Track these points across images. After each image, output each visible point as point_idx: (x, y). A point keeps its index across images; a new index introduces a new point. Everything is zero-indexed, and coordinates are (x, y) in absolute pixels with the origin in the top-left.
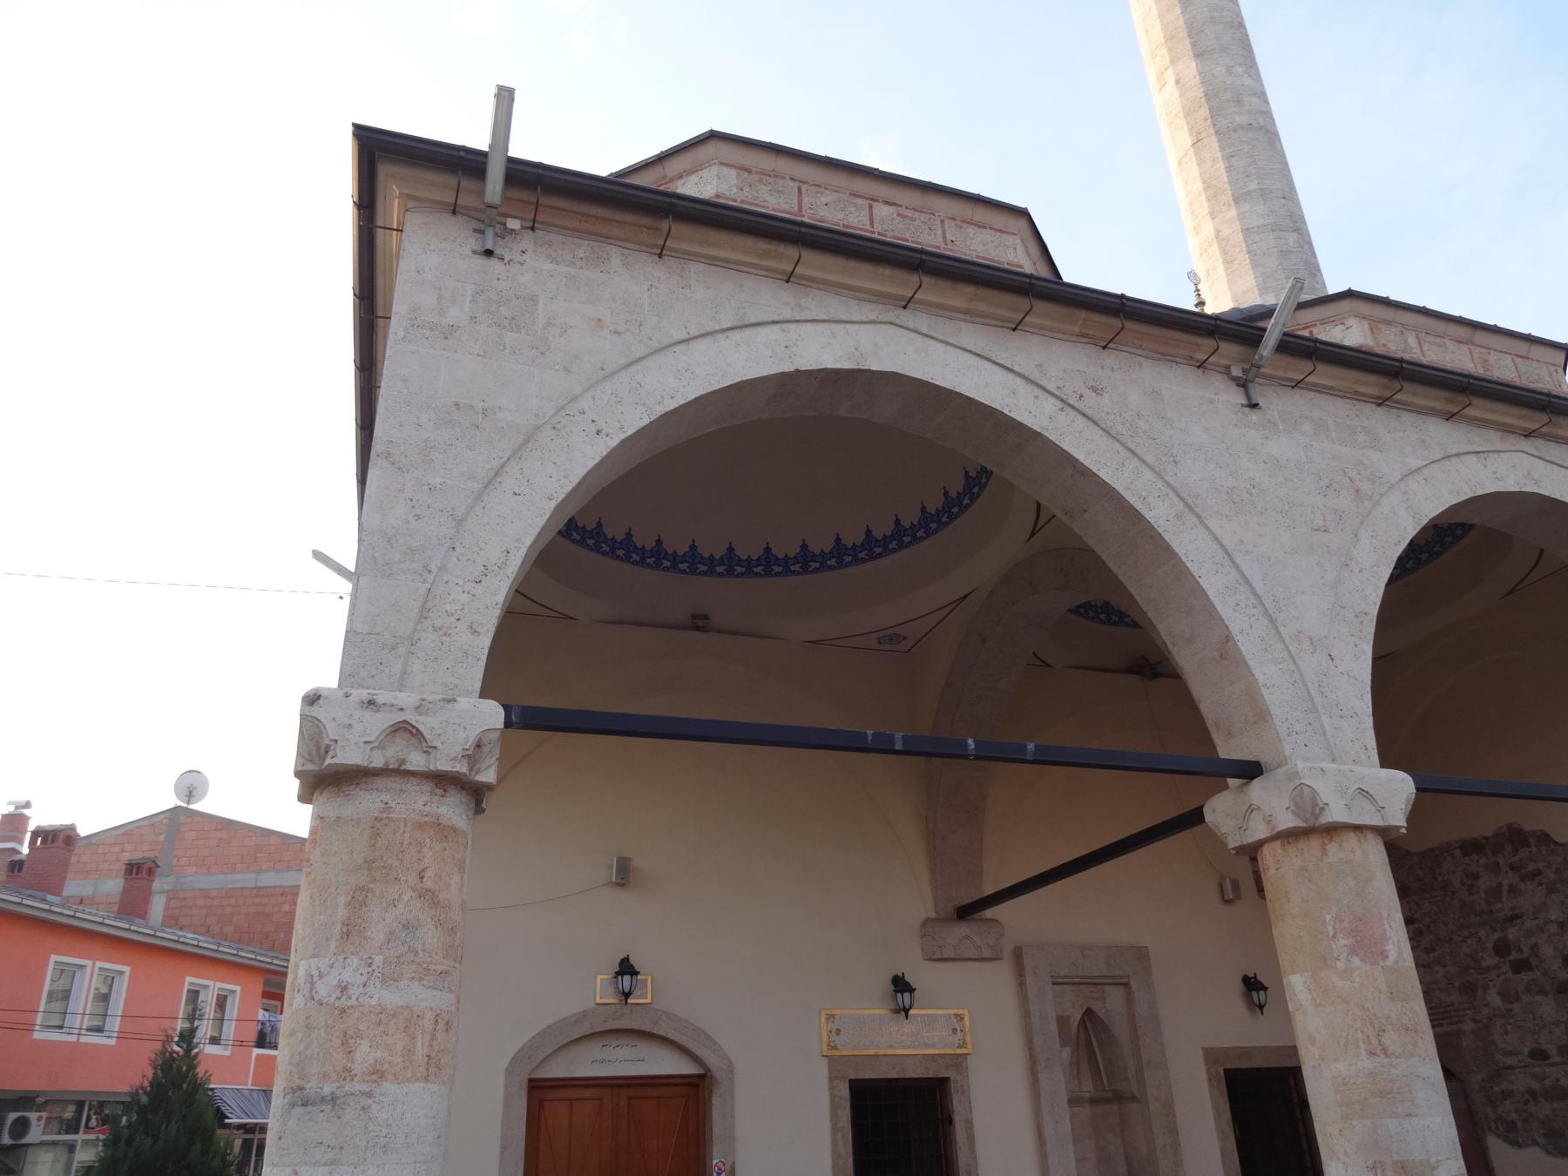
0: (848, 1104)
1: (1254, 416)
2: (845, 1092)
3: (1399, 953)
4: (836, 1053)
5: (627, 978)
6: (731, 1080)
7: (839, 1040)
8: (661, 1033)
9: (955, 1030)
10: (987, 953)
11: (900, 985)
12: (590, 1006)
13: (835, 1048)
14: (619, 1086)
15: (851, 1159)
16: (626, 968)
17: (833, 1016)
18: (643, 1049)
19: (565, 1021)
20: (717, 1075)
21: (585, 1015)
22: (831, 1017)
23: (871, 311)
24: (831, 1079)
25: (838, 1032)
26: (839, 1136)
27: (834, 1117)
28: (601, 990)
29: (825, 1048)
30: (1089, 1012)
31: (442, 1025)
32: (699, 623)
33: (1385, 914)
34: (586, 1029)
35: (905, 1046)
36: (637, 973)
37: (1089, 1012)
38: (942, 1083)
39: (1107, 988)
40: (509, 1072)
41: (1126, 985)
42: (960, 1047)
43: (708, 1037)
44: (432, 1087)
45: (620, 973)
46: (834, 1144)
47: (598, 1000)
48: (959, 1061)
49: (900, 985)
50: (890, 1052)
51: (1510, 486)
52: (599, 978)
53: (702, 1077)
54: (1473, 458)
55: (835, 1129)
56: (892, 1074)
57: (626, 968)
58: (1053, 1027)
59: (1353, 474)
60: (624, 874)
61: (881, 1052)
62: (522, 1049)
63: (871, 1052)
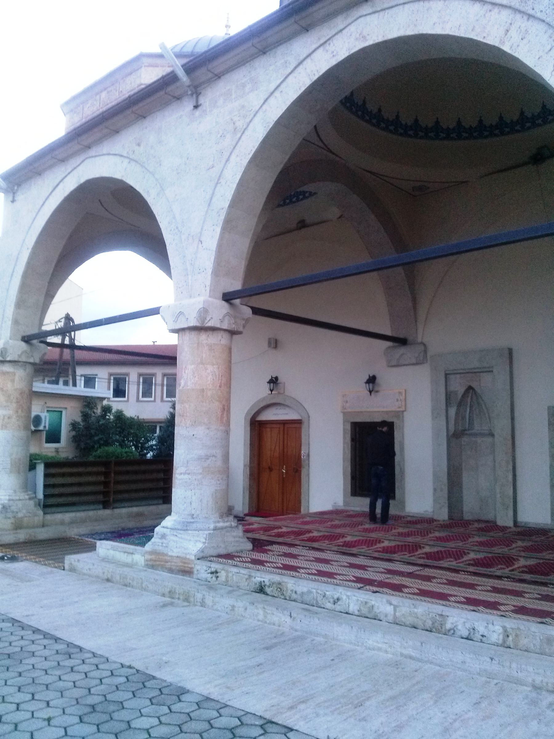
0: (350, 433)
1: (197, 113)
2: (349, 427)
3: (186, 383)
4: (345, 411)
5: (272, 384)
8: (286, 404)
9: (397, 400)
10: (414, 361)
11: (372, 380)
13: (345, 409)
15: (350, 455)
16: (274, 381)
18: (287, 410)
20: (303, 420)
23: (82, 157)
24: (344, 422)
27: (344, 438)
30: (470, 388)
31: (6, 418)
32: (302, 225)
33: (184, 367)
35: (375, 408)
37: (470, 388)
38: (390, 425)
39: (481, 374)
40: (245, 419)
41: (492, 371)
42: (399, 407)
44: (5, 431)
46: (344, 449)
48: (399, 414)
49: (372, 380)
50: (368, 410)
51: (343, 55)
54: (321, 48)
55: (344, 443)
56: (368, 420)
57: (274, 381)
58: (443, 397)
59: (236, 119)
63: (359, 410)
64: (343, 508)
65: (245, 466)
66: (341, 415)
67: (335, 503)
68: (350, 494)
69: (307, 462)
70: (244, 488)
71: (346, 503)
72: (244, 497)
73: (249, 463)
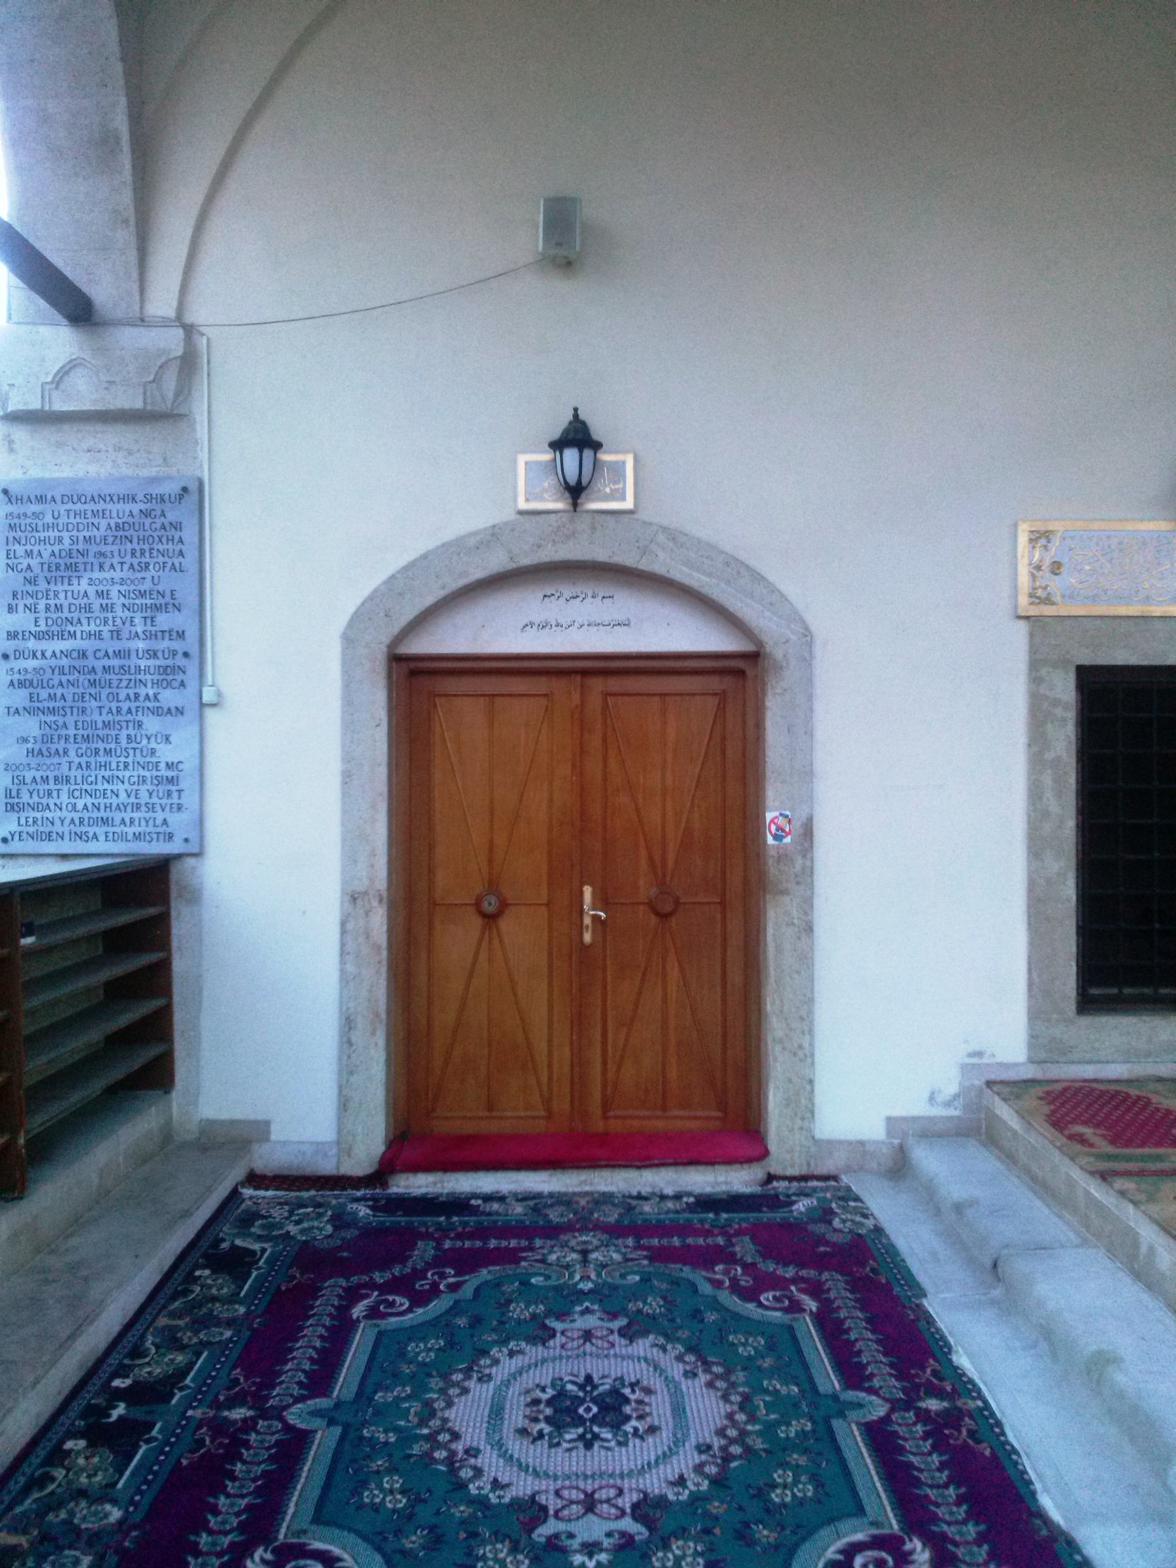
2: (1065, 689)
4: (1048, 610)
5: (571, 455)
6: (807, 661)
7: (1056, 585)
8: (658, 568)
12: (508, 515)
13: (1048, 601)
14: (585, 673)
16: (578, 437)
17: (1047, 535)
18: (626, 603)
19: (456, 547)
20: (778, 653)
21: (494, 534)
22: (1040, 537)
24: (1035, 664)
25: (1056, 568)
26: (1047, 779)
28: (525, 482)
29: (1023, 600)
34: (496, 562)
36: (596, 446)
40: (348, 640)
43: (758, 578)
45: (558, 445)
46: (1035, 794)
47: (523, 505)
52: (522, 459)
53: (754, 657)
57: (578, 437)
60: (568, 243)
61: (1157, 611)
62: (371, 598)
64: (1030, 1072)
65: (353, 898)
66: (1022, 627)
67: (979, 1054)
68: (1071, 1005)
69: (799, 862)
70: (348, 1023)
71: (1041, 1045)
72: (347, 1068)
73: (381, 883)
